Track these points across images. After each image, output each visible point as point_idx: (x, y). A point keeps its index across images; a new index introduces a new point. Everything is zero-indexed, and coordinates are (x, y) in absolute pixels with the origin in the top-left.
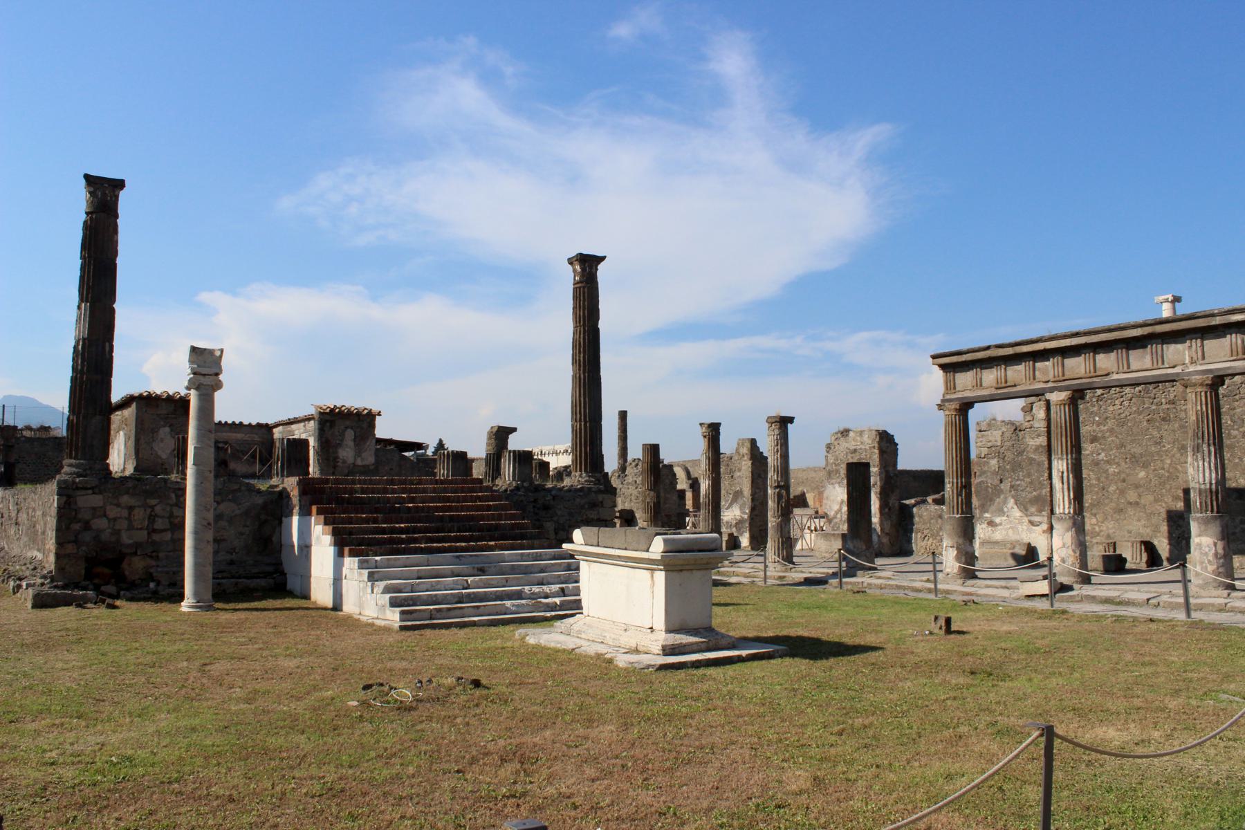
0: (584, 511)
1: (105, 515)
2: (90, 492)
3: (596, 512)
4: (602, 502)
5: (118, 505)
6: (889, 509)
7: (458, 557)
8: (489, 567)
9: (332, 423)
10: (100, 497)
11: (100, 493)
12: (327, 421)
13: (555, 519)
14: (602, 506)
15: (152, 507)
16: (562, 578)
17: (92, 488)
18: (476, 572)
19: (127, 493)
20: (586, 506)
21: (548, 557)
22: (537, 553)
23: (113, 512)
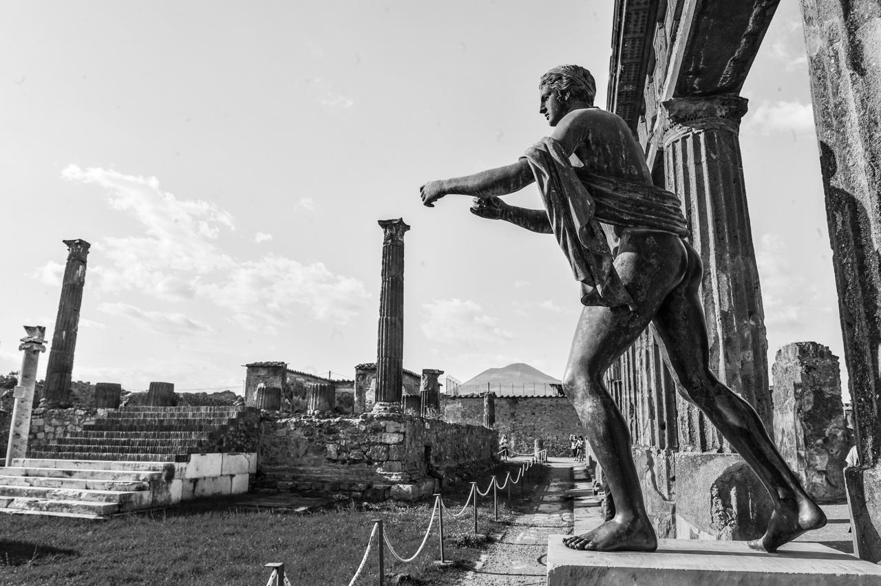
0: (366, 435)
1: (44, 431)
2: (38, 417)
3: (379, 437)
4: (385, 427)
5: (50, 425)
6: (826, 441)
7: (76, 463)
8: (75, 472)
9: (364, 376)
10: (42, 420)
11: (43, 417)
12: (360, 374)
13: (338, 442)
14: (385, 431)
15: (66, 426)
16: (106, 485)
17: (40, 415)
18: (60, 474)
19: (55, 417)
20: (369, 431)
21: (144, 468)
22: (136, 465)
23: (47, 429)
